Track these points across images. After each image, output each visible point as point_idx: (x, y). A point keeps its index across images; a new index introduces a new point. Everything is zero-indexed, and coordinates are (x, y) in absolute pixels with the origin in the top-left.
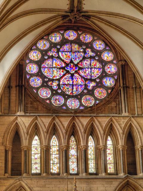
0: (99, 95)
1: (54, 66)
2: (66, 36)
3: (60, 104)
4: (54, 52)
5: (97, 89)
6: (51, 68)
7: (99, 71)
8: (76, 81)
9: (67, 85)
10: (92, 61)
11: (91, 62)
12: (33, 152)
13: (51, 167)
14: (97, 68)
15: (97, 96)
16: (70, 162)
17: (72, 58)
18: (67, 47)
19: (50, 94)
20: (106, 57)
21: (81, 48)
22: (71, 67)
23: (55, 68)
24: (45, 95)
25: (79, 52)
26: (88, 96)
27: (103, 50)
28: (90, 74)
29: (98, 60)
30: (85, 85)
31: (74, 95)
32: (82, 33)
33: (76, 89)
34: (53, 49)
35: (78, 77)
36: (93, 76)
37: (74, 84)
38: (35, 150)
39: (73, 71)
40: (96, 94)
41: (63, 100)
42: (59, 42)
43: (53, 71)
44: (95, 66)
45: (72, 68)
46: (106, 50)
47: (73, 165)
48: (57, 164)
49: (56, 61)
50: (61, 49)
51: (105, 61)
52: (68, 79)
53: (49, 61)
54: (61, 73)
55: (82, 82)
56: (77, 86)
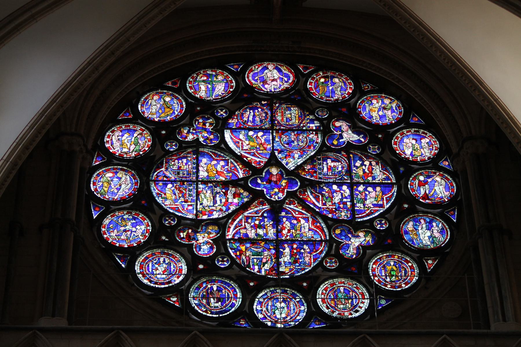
1: (203, 174)
2: (253, 82)
3: (226, 311)
4: (205, 130)
7: (384, 193)
8: (293, 226)
9: (254, 242)
10: (355, 161)
11: (349, 166)
14: (374, 185)
15: (379, 281)
17: (273, 150)
18: (254, 116)
20: (411, 150)
21: (311, 117)
22: (269, 181)
25: (299, 130)
26: (340, 280)
28: (349, 204)
29: (378, 157)
30: (330, 242)
32: (316, 71)
33: (291, 256)
34: (201, 121)
36: (360, 212)
37: (284, 238)
39: (280, 195)
41: (236, 296)
43: (198, 194)
45: (276, 182)
46: (409, 126)
50: (230, 121)
52: (257, 222)
53: (185, 161)
54: (230, 201)
56: (295, 246)
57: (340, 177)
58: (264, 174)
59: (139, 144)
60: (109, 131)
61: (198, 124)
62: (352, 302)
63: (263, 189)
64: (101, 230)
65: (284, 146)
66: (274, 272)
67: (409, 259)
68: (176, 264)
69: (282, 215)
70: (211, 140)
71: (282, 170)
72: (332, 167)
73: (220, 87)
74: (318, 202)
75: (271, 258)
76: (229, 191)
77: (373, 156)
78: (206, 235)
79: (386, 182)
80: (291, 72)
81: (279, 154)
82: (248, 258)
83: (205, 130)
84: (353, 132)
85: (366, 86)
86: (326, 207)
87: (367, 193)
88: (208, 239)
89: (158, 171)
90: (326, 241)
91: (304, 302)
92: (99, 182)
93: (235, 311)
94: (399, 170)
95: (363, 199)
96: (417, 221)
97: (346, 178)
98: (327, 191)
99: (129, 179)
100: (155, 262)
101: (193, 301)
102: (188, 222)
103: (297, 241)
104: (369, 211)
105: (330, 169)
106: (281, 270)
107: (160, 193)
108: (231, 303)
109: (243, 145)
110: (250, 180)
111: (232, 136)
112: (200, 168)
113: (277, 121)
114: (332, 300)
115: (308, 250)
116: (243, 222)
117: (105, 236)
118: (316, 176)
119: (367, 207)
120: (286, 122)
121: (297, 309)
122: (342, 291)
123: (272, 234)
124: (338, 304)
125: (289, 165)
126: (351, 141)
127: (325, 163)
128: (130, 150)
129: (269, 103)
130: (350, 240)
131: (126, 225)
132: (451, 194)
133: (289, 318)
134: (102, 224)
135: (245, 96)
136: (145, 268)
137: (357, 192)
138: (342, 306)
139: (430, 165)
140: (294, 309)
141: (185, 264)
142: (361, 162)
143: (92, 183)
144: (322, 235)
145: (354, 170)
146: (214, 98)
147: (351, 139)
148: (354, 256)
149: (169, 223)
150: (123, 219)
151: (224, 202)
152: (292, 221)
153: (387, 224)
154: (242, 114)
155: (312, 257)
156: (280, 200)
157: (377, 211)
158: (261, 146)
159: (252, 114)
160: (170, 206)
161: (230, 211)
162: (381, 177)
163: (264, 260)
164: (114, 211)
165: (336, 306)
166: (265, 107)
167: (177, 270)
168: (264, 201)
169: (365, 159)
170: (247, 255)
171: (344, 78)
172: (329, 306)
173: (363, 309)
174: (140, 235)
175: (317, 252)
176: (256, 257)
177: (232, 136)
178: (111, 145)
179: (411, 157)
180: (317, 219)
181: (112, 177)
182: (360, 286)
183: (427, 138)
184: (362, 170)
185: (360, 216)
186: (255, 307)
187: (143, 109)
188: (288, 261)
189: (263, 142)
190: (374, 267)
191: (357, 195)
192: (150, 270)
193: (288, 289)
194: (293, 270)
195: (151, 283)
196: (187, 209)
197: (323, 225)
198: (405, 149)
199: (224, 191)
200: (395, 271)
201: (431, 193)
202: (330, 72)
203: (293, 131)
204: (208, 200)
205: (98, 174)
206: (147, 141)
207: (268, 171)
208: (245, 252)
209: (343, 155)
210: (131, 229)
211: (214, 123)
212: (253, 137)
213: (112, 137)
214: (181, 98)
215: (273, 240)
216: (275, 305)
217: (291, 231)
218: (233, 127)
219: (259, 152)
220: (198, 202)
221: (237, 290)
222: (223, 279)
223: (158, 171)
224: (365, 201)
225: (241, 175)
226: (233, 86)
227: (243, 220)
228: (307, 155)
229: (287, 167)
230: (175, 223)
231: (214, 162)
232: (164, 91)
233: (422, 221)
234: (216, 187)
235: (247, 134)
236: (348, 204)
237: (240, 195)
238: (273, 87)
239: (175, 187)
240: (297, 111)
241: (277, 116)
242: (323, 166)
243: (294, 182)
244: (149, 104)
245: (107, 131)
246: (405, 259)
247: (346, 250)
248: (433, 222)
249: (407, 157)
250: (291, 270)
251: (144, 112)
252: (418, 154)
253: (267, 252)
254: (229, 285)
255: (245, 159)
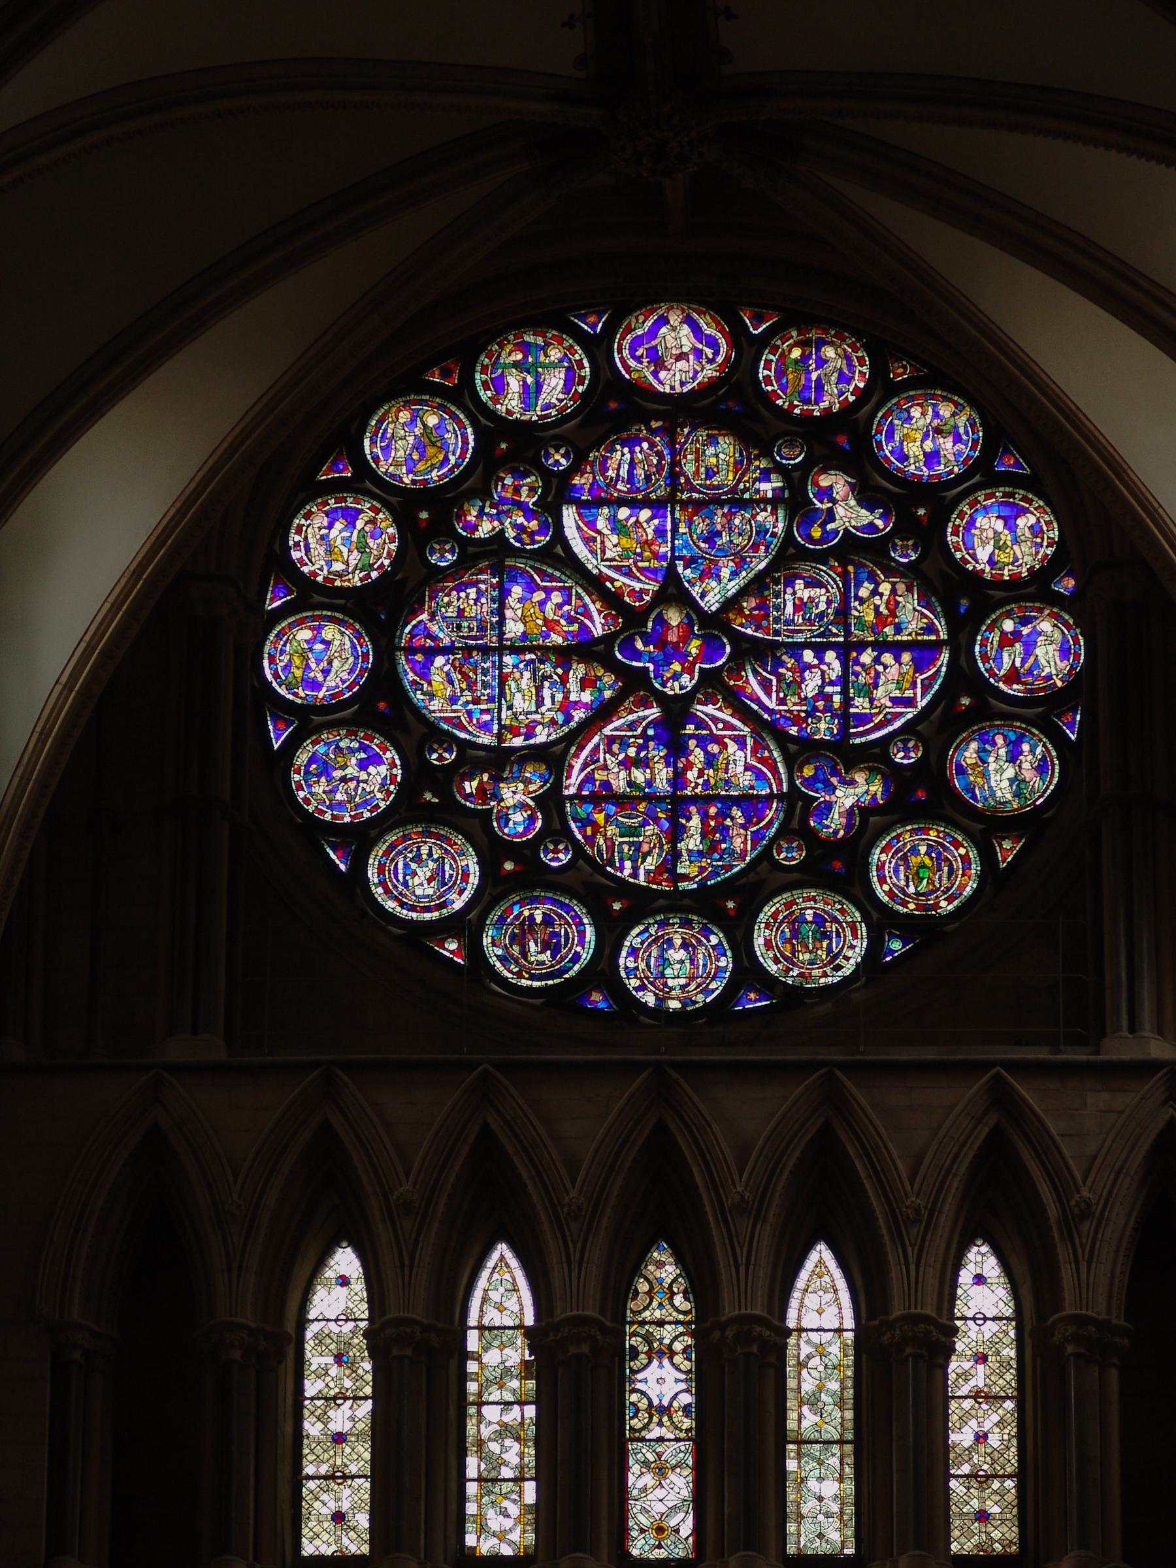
0: (911, 890)
1: (514, 629)
2: (632, 363)
4: (522, 506)
5: (897, 837)
6: (485, 650)
7: (919, 667)
8: (711, 759)
9: (624, 802)
10: (859, 585)
12: (311, 1388)
13: (471, 1508)
14: (897, 649)
15: (891, 894)
16: (635, 1469)
17: (674, 558)
18: (632, 465)
19: (474, 880)
20: (989, 548)
21: (763, 464)
23: (515, 650)
24: (422, 886)
25: (738, 502)
27: (960, 479)
28: (837, 699)
29: (912, 574)
31: (683, 885)
33: (704, 835)
34: (508, 481)
35: (728, 726)
36: (863, 719)
37: (688, 792)
38: (334, 1371)
39: (685, 679)
40: (882, 880)
41: (582, 935)
42: (563, 420)
43: (503, 679)
44: (889, 630)
46: (993, 480)
47: (660, 1493)
48: (519, 1480)
49: (531, 587)
50: (577, 481)
51: (977, 575)
53: (472, 592)
55: (760, 775)
57: (822, 629)
58: (650, 624)
59: (368, 550)
60: (299, 516)
61: (504, 486)
62: (830, 946)
63: (647, 665)
64: (289, 779)
65: (698, 547)
66: (665, 876)
67: (960, 839)
68: (456, 861)
69: (687, 732)
70: (532, 535)
71: (691, 612)
72: (805, 600)
73: (553, 382)
74: (769, 695)
75: (660, 842)
76: (572, 672)
77: (901, 569)
78: (521, 786)
79: (925, 638)
80: (722, 331)
81: (685, 568)
82: (609, 843)
83: (522, 506)
84: (860, 503)
85: (899, 367)
86: (785, 708)
87: (880, 668)
88: (524, 797)
89: (414, 622)
90: (781, 797)
91: (727, 948)
92: (281, 654)
93: (581, 973)
94: (958, 605)
95: (870, 684)
96: (986, 741)
97: (835, 631)
98: (789, 666)
99: (348, 644)
100: (410, 855)
101: (490, 949)
102: (482, 753)
103: (718, 798)
104: (881, 716)
105: (800, 606)
106: (680, 870)
107: (418, 680)
108: (573, 951)
109: (604, 547)
110: (618, 642)
111: (580, 522)
112: (509, 613)
113: (685, 476)
114: (789, 941)
115: (741, 821)
116: (601, 751)
117: (301, 794)
118: (768, 628)
119: (879, 705)
120: (706, 479)
121: (711, 964)
122: (809, 918)
123: (665, 781)
124: (798, 951)
125: (707, 599)
126: (854, 527)
127: (789, 590)
128: (348, 565)
129: (667, 425)
130: (834, 793)
131: (344, 767)
132: (1072, 665)
133: (693, 986)
134: (292, 765)
135: (613, 405)
136: (389, 871)
137: (858, 668)
138: (807, 956)
139: (1032, 589)
140: (705, 965)
141: (475, 860)
142: (871, 587)
143: (266, 656)
144: (773, 781)
145: (856, 609)
146: (539, 413)
147: (853, 523)
148: (842, 833)
149: (440, 758)
150: (339, 749)
151: (560, 700)
152: (709, 748)
153: (918, 750)
154: (606, 459)
155: (749, 837)
156: (683, 691)
157: (901, 714)
158: (646, 546)
159: (628, 456)
160: (442, 715)
161: (573, 724)
162: (914, 626)
163: (645, 848)
164: (318, 729)
165: (794, 955)
166: (658, 438)
167: (458, 874)
168: (649, 697)
169: (883, 577)
170: (609, 833)
171: (848, 345)
172: (779, 956)
173: (852, 961)
174: (376, 790)
175: (761, 825)
176: (627, 839)
177: (580, 522)
178: (306, 555)
179: (988, 569)
180: (764, 740)
181: (311, 639)
182: (850, 906)
183: (1032, 513)
184: (872, 607)
185: (861, 729)
186: (622, 961)
187: (375, 450)
188: (696, 849)
189: (650, 537)
190: (882, 859)
191: (857, 674)
192: (401, 880)
193: (695, 918)
194: (707, 869)
195: (403, 908)
196: (478, 720)
197: (776, 754)
198: (976, 547)
199: (560, 671)
200: (928, 868)
201: (1027, 666)
202: (817, 328)
203: (722, 504)
204: (526, 697)
205: (279, 632)
206: (387, 541)
207: (660, 615)
208: (605, 827)
209: (832, 568)
210: (357, 775)
211: (539, 487)
212: (629, 524)
213: (306, 531)
214: (462, 416)
215: (665, 797)
216: (666, 956)
217: (706, 772)
218: (583, 498)
219: (640, 564)
220: (503, 702)
221: (586, 921)
222: (555, 894)
223: (414, 622)
224: (875, 692)
225: (598, 631)
226: (584, 378)
227: (602, 747)
228: (749, 570)
229: (702, 604)
230: (453, 757)
231: (539, 595)
232: (424, 397)
233: (999, 740)
234: (542, 662)
235: (615, 516)
236: (834, 700)
237: (596, 681)
238: (678, 377)
239: (453, 665)
240: (732, 447)
241: (684, 461)
242: (784, 600)
243: (717, 644)
244: (389, 436)
245: (294, 516)
246: (953, 837)
247: (825, 817)
248: (1022, 743)
249: (979, 567)
250: (702, 870)
251: (376, 459)
252: (1006, 560)
253: (652, 827)
254: (568, 909)
255: (608, 584)
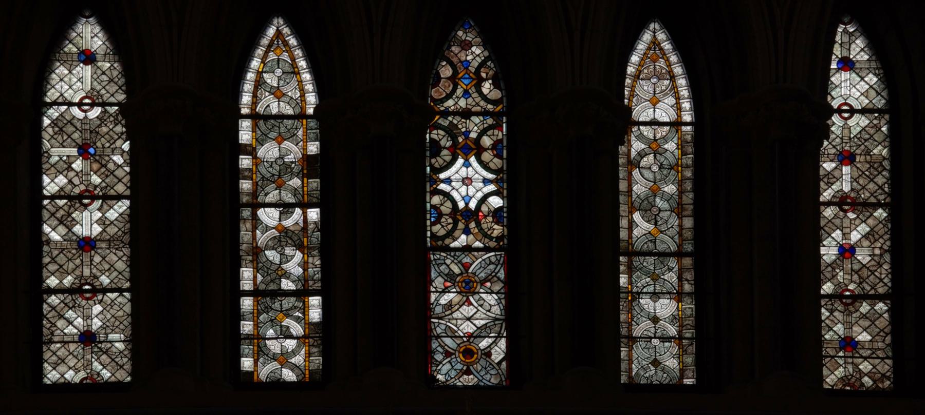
12: (51, 184)
13: (247, 327)
16: (439, 283)
38: (78, 165)
47: (467, 311)
48: (302, 294)
